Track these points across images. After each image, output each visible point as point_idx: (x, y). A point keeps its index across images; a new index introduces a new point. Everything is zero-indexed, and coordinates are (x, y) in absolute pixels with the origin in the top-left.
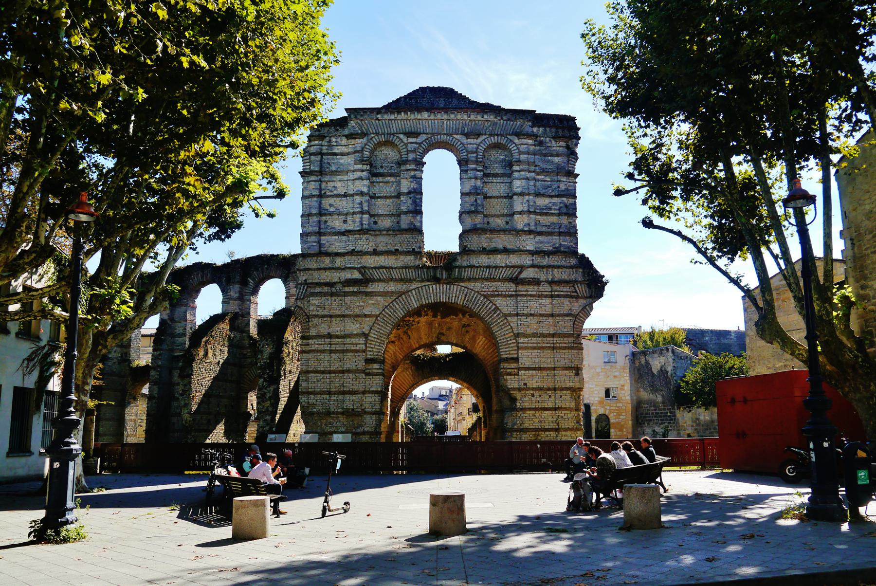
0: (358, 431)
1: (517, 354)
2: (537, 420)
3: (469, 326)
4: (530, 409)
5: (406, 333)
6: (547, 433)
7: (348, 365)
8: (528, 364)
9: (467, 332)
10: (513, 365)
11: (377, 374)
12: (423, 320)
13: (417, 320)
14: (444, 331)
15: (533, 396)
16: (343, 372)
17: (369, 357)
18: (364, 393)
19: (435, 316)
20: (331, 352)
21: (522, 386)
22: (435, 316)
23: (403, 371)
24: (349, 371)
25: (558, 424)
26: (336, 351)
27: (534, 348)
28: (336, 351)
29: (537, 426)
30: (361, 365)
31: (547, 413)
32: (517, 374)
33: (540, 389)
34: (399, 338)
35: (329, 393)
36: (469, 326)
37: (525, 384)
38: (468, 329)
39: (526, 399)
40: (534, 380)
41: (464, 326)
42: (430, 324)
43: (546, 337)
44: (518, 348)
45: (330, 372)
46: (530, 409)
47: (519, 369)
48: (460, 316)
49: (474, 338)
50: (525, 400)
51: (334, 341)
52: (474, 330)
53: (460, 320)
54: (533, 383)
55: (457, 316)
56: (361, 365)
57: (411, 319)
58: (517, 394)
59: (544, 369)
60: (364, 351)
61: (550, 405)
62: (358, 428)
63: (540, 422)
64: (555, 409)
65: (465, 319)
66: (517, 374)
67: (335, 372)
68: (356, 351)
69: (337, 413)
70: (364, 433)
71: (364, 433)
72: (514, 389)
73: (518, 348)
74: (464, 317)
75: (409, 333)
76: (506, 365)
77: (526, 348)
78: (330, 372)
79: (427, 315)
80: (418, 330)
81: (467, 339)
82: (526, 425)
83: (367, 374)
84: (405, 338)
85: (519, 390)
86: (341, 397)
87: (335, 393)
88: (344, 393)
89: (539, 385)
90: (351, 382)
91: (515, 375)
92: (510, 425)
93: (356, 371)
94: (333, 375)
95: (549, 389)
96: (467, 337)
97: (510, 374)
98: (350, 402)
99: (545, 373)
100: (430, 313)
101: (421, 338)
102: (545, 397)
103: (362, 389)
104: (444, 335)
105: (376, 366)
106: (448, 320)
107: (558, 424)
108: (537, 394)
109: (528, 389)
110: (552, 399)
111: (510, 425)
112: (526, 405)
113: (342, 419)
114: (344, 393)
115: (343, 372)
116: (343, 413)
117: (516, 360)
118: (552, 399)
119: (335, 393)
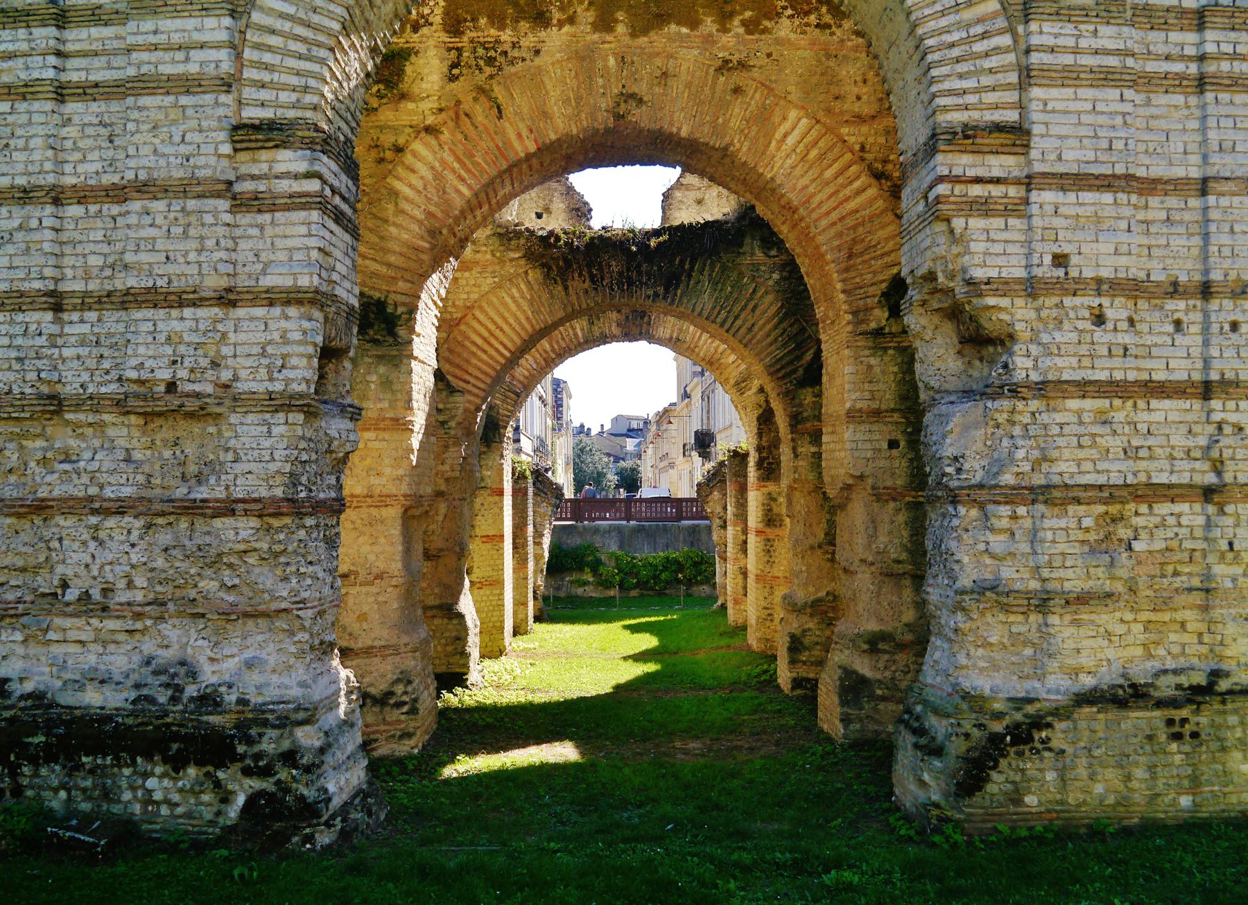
0: (202, 493)
1: (1021, 106)
2: (1116, 444)
3: (742, 65)
4: (1084, 388)
5: (482, 91)
6: (1163, 508)
7: (147, 154)
8: (1074, 158)
9: (737, 91)
10: (999, 165)
11: (298, 202)
12: (555, 39)
13: (528, 41)
14: (641, 89)
15: (1099, 320)
16: (118, 194)
17: (252, 114)
18: (227, 299)
19: (604, 24)
20: (61, 93)
21: (1046, 271)
22: (604, 24)
23: (499, 286)
24: (145, 188)
25: (1218, 467)
26: (88, 91)
27: (1106, 78)
28: (88, 91)
29: (1116, 471)
30: (212, 155)
31: (1165, 408)
32: (1020, 208)
33: (1134, 289)
34: (456, 112)
35: (56, 303)
36: (742, 65)
37: (1060, 260)
38: (737, 78)
39: (1065, 336)
40: (1107, 240)
41: (725, 66)
42: (584, 58)
43: (1165, 26)
44: (1027, 77)
45: (57, 197)
46: (1084, 388)
47: (1029, 182)
48: (709, 25)
49: (763, 119)
50: (1048, 343)
51: (77, 38)
52: (767, 87)
53: (708, 40)
54: (1098, 257)
55: (694, 24)
56: (212, 155)
57: (507, 36)
58: (1016, 313)
59: (1151, 186)
60: (227, 84)
61: (1182, 369)
62: (200, 479)
63: (1130, 453)
64: (1206, 390)
65: (727, 40)
66: (1020, 208)
67: (83, 196)
68: (188, 85)
69: (94, 403)
70: (228, 508)
71: (228, 508)
72: (1003, 287)
73: (1027, 77)
74: (724, 30)
75: (499, 92)
76: (964, 163)
77: (1069, 77)
78: (57, 197)
79: (571, 20)
80: (536, 80)
81: (735, 123)
82: (1065, 468)
83: (241, 204)
84: (480, 112)
85: (1032, 288)
86: (113, 321)
87: (87, 302)
88: (128, 300)
89: (1133, 267)
90: (160, 244)
91: (1008, 211)
92: (975, 470)
93: (184, 189)
94: (75, 210)
95: (1175, 289)
96: (737, 114)
97: (984, 208)
98: (154, 347)
99: (1157, 207)
100: (586, 16)
101: (546, 115)
102: (1155, 322)
103: (213, 283)
104: (640, 101)
105: (290, 160)
106: (658, 40)
107: (1218, 467)
108: (1116, 310)
109: (1074, 287)
110: (1192, 339)
111: (975, 470)
112: (1066, 368)
113: (124, 432)
114: (128, 300)
115: (118, 194)
116: (121, 405)
117: (1016, 135)
118: (1192, 339)
119: (87, 302)
